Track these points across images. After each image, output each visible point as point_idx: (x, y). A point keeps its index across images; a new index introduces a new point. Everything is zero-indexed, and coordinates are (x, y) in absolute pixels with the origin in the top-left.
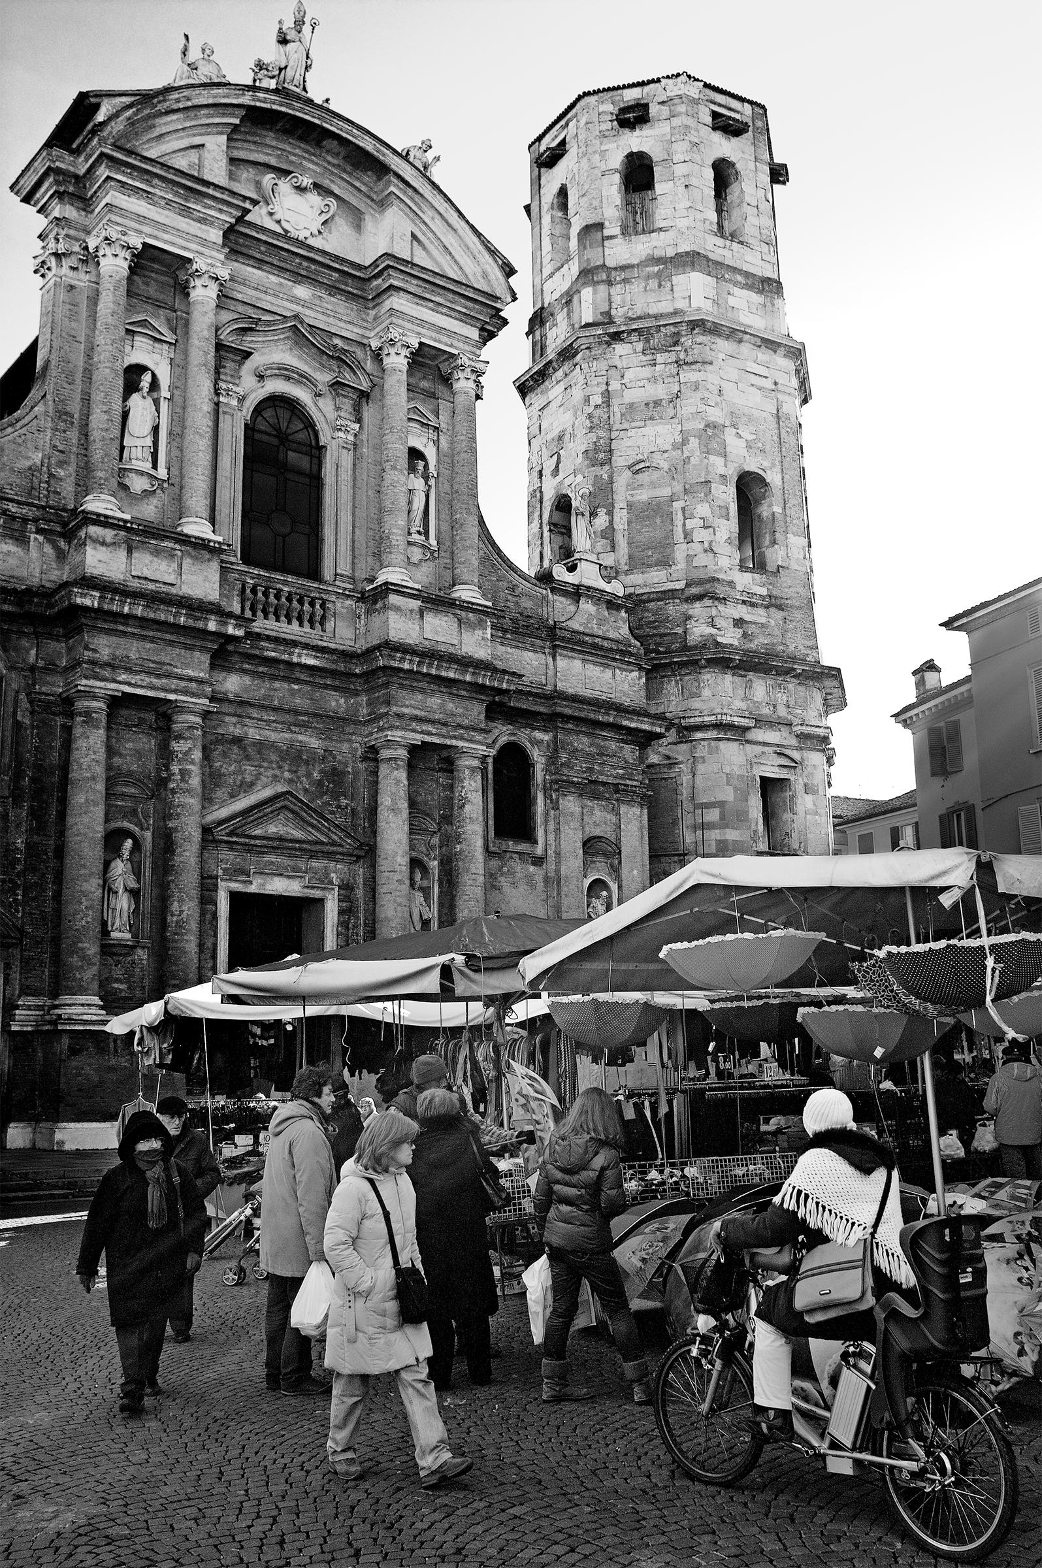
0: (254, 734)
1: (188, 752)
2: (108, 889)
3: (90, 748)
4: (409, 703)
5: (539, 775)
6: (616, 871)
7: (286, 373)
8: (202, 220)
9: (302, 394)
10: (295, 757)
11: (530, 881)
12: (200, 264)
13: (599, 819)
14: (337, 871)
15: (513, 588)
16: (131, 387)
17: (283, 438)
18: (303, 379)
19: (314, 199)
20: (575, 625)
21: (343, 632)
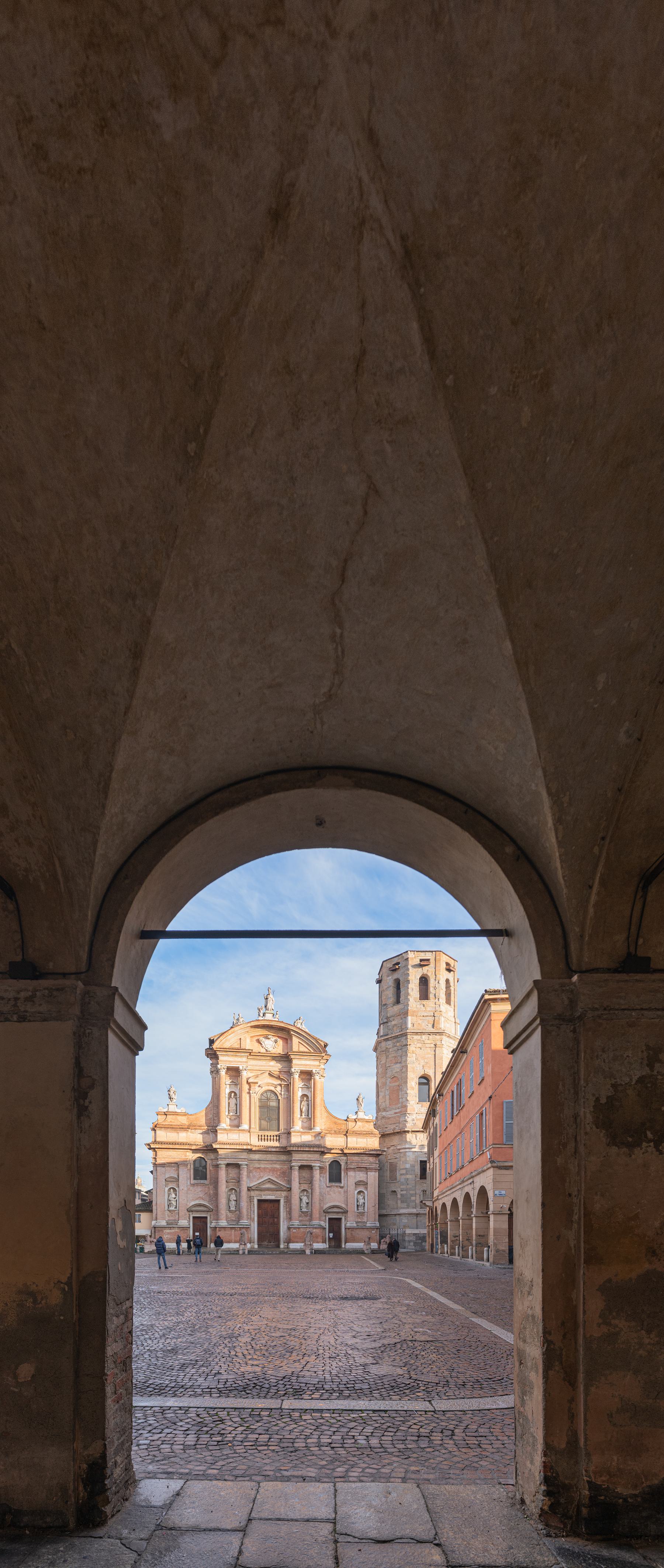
0: (263, 1166)
1: (244, 1173)
2: (229, 1200)
3: (223, 1174)
4: (296, 1156)
5: (343, 1167)
6: (366, 1188)
7: (268, 1084)
8: (241, 1057)
9: (272, 1088)
10: (273, 1170)
11: (340, 1193)
12: (241, 1068)
13: (361, 1176)
14: (284, 1194)
15: (335, 1123)
16: (230, 1097)
17: (268, 1099)
18: (272, 1085)
19: (274, 1039)
20: (355, 1129)
21: (284, 1143)
